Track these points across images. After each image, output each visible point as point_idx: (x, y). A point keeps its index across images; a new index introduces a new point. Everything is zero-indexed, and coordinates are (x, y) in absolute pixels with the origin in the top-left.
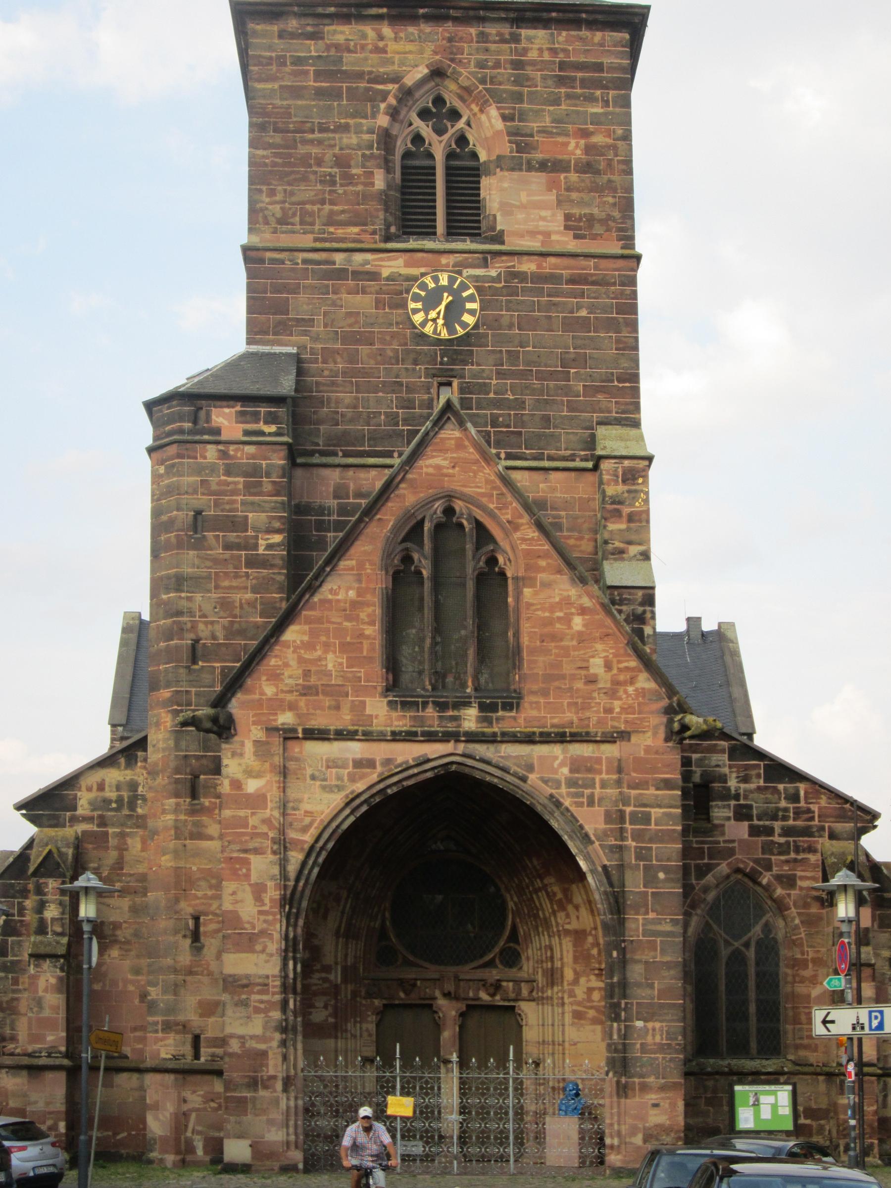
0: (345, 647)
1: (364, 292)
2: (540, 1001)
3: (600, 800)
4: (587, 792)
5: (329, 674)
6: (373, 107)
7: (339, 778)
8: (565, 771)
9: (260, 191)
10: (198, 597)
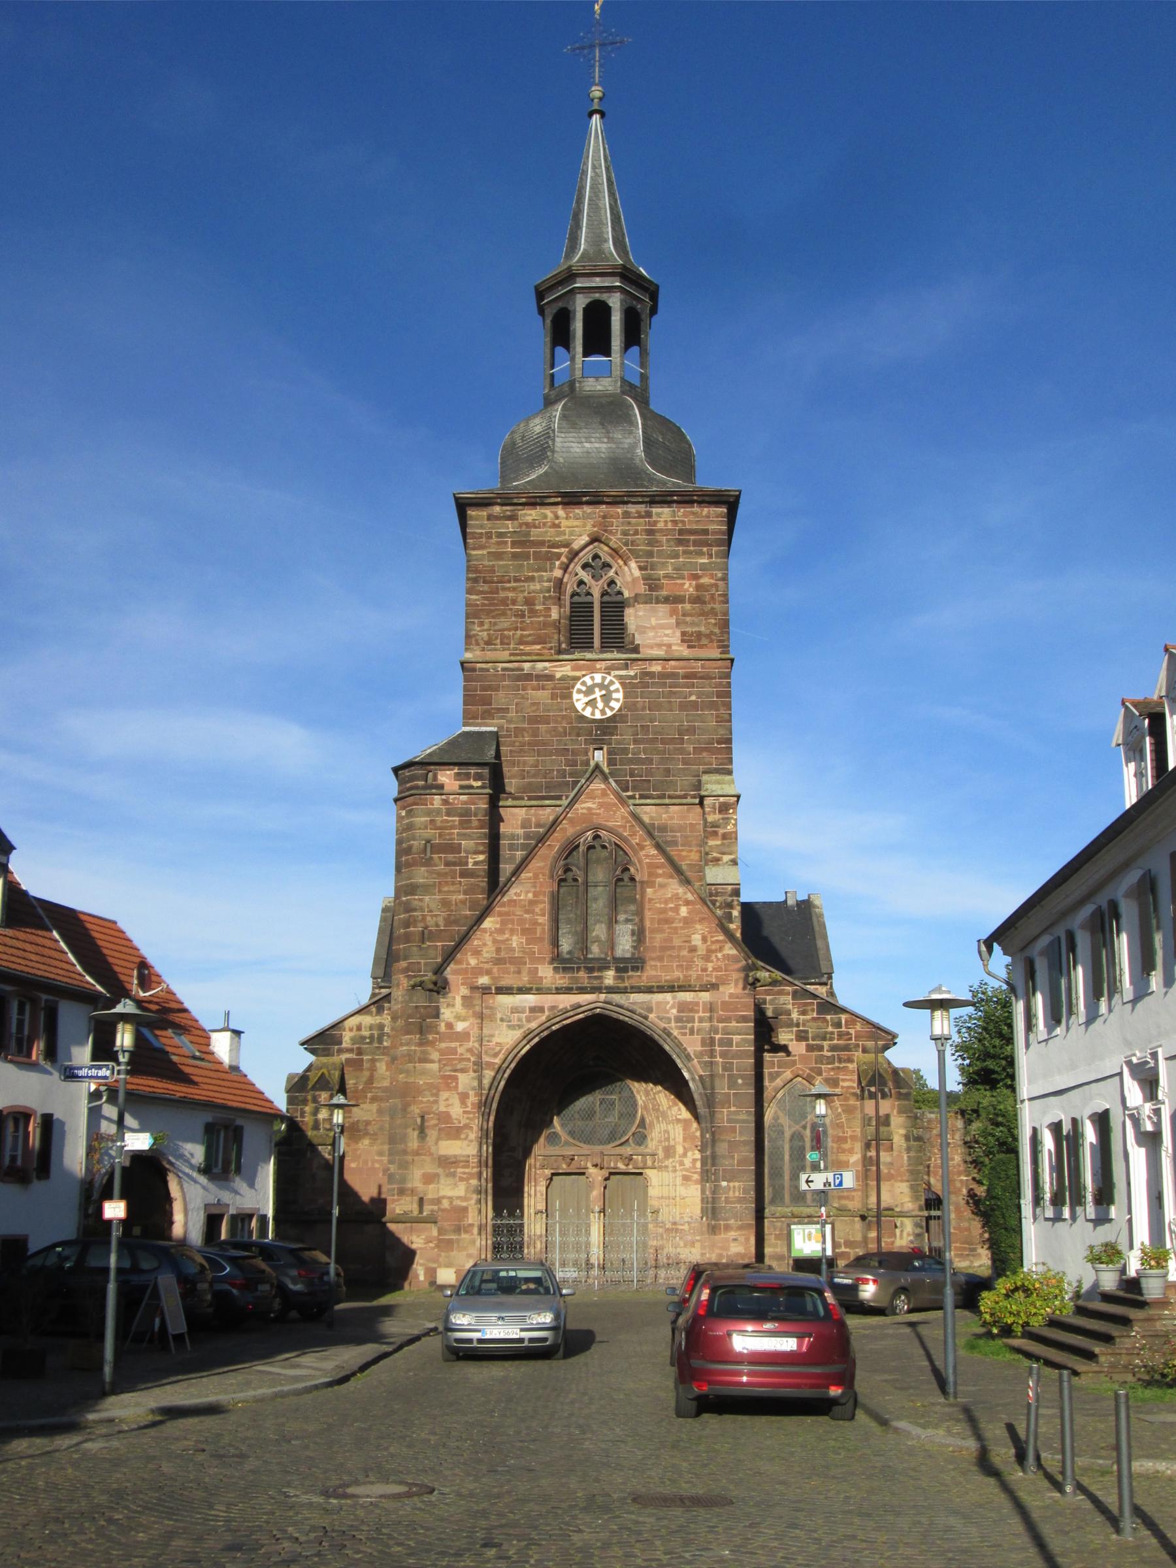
0: (524, 932)
2: (660, 1168)
3: (698, 1030)
4: (689, 1025)
5: (513, 950)
7: (520, 1020)
8: (674, 1011)
10: (427, 898)
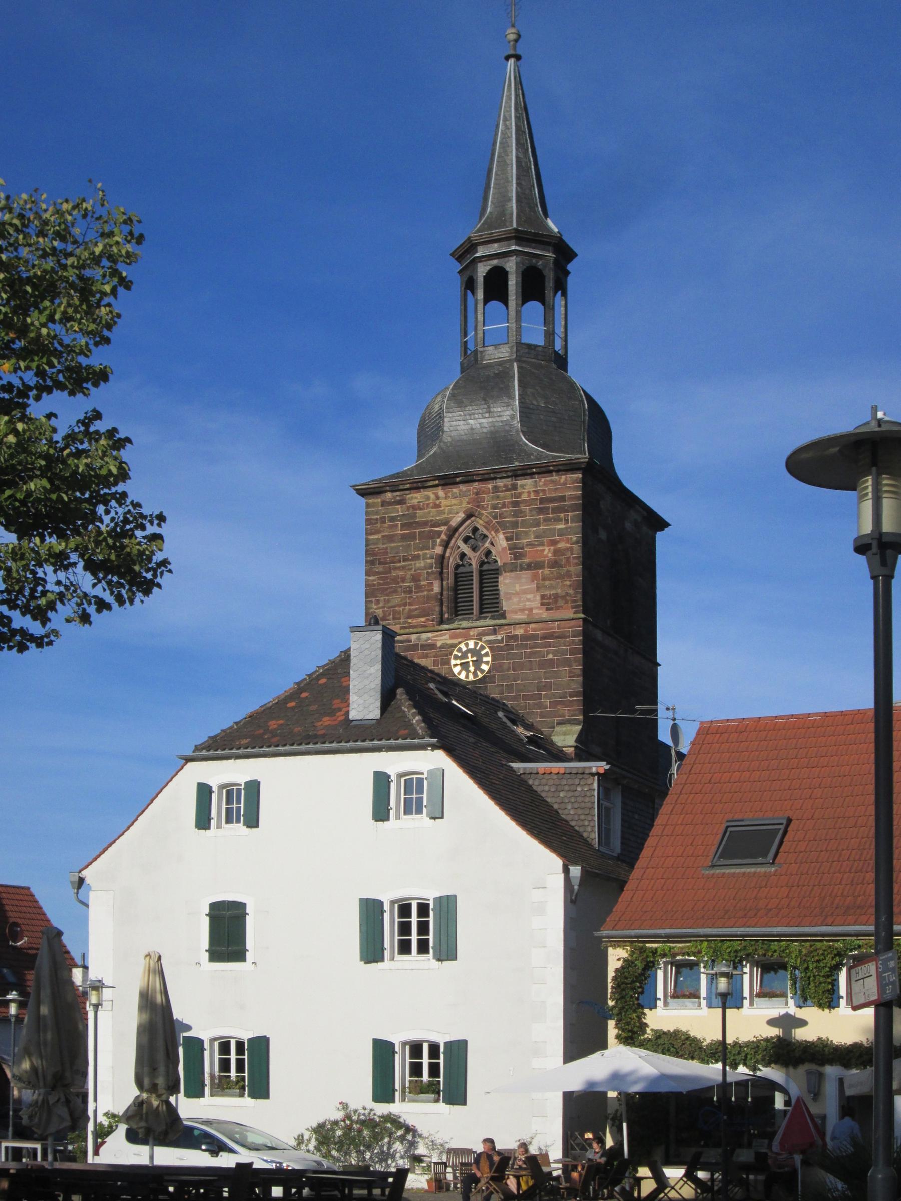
1: (427, 657)
6: (433, 542)
9: (371, 601)
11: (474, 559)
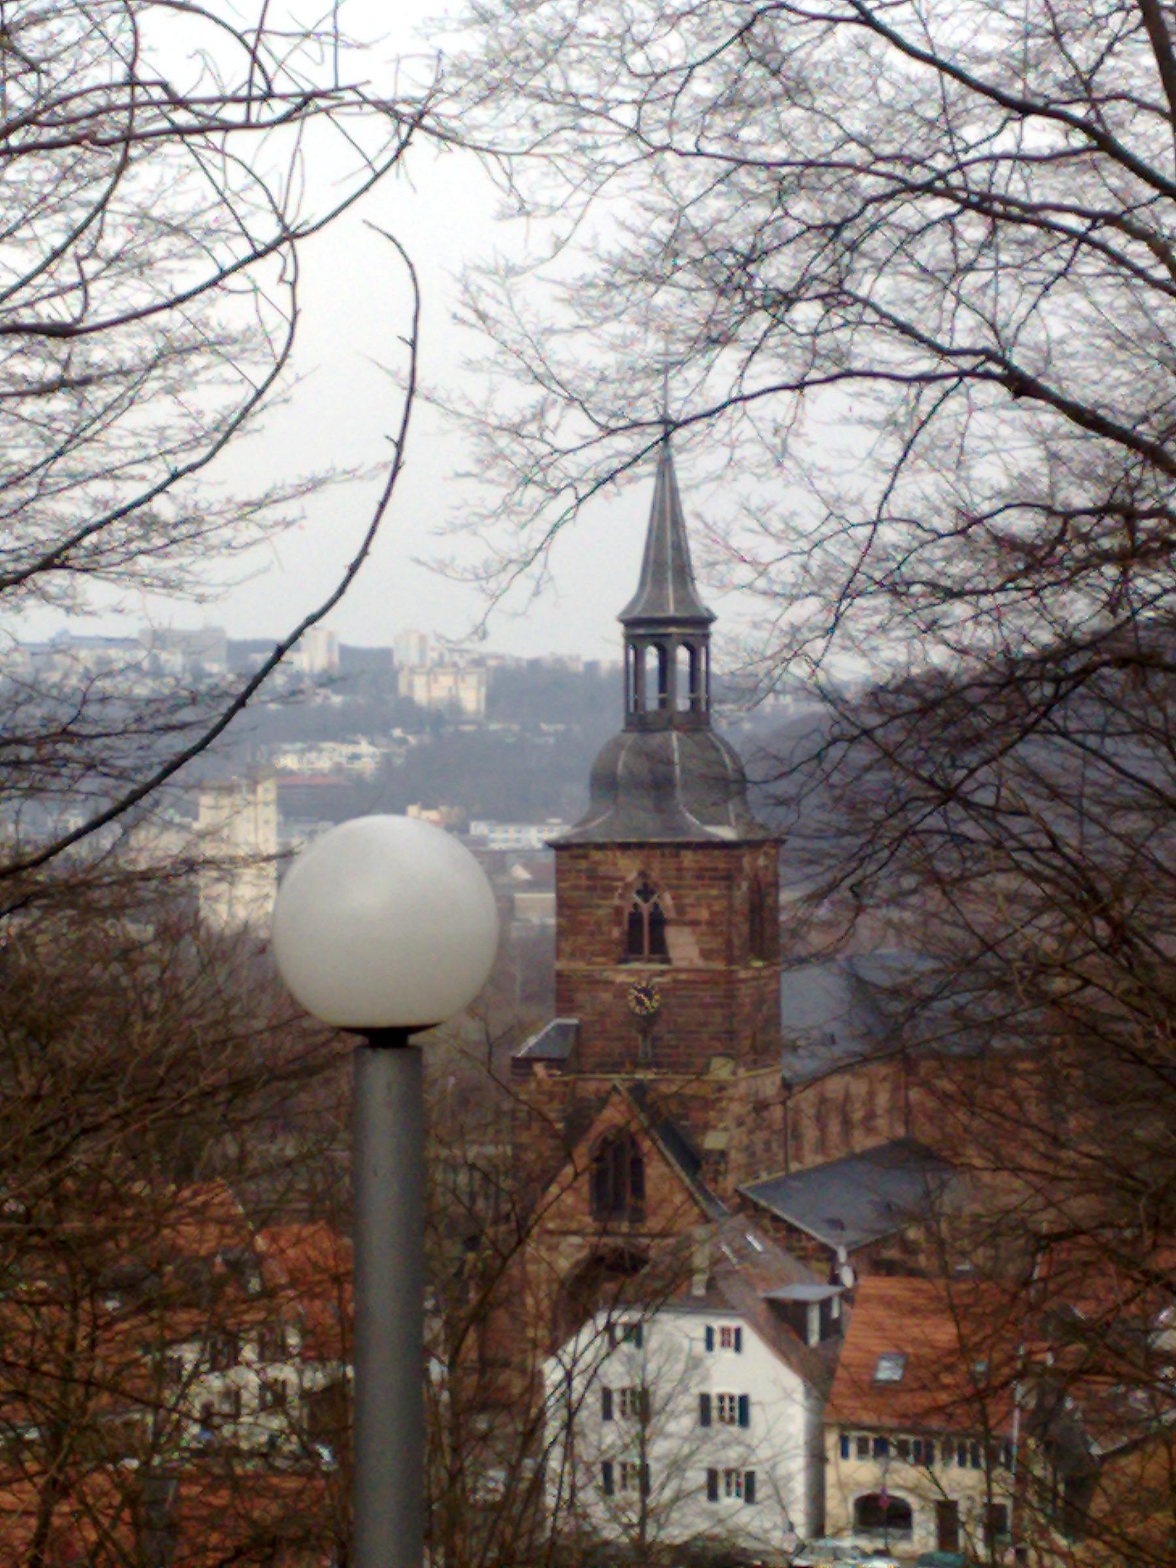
11: (646, 909)
